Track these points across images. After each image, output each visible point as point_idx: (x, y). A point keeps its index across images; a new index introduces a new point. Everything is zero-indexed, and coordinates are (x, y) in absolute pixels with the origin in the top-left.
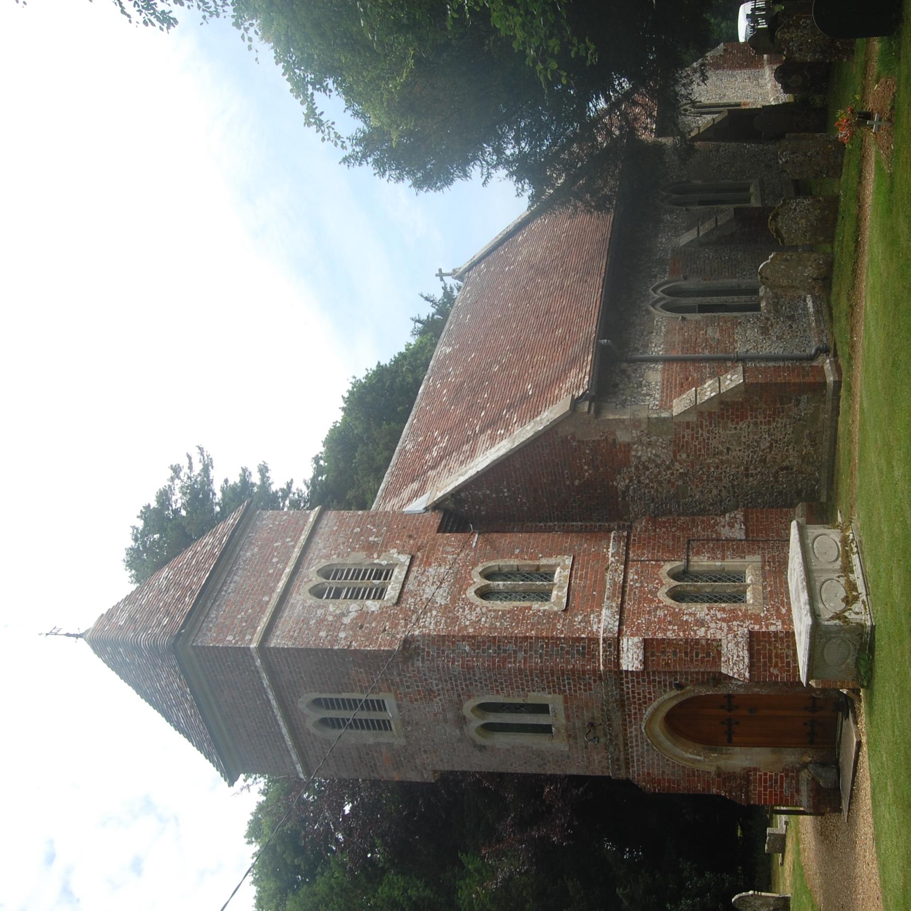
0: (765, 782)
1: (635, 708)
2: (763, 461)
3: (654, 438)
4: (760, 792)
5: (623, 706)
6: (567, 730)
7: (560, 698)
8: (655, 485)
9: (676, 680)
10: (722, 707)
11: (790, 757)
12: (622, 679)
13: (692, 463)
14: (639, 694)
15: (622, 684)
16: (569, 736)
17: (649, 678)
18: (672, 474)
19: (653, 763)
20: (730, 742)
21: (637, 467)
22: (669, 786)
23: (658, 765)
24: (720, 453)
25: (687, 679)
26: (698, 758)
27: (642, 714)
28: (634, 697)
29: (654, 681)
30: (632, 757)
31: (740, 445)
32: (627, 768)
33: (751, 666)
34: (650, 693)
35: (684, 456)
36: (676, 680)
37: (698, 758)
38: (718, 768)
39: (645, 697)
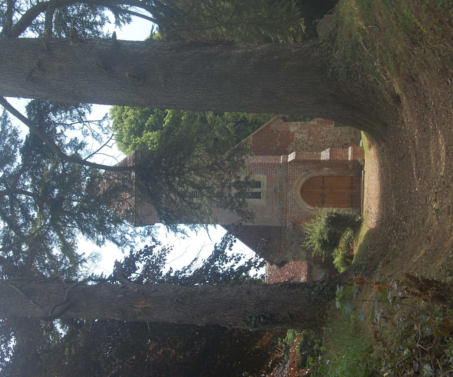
2: (338, 141)
3: (302, 130)
5: (287, 181)
6: (266, 194)
7: (266, 176)
8: (301, 150)
10: (321, 188)
13: (314, 141)
16: (267, 197)
18: (308, 146)
21: (296, 142)
23: (297, 212)
24: (324, 137)
26: (312, 208)
27: (293, 185)
31: (330, 134)
32: (286, 214)
33: (330, 156)
35: (312, 138)
37: (312, 208)
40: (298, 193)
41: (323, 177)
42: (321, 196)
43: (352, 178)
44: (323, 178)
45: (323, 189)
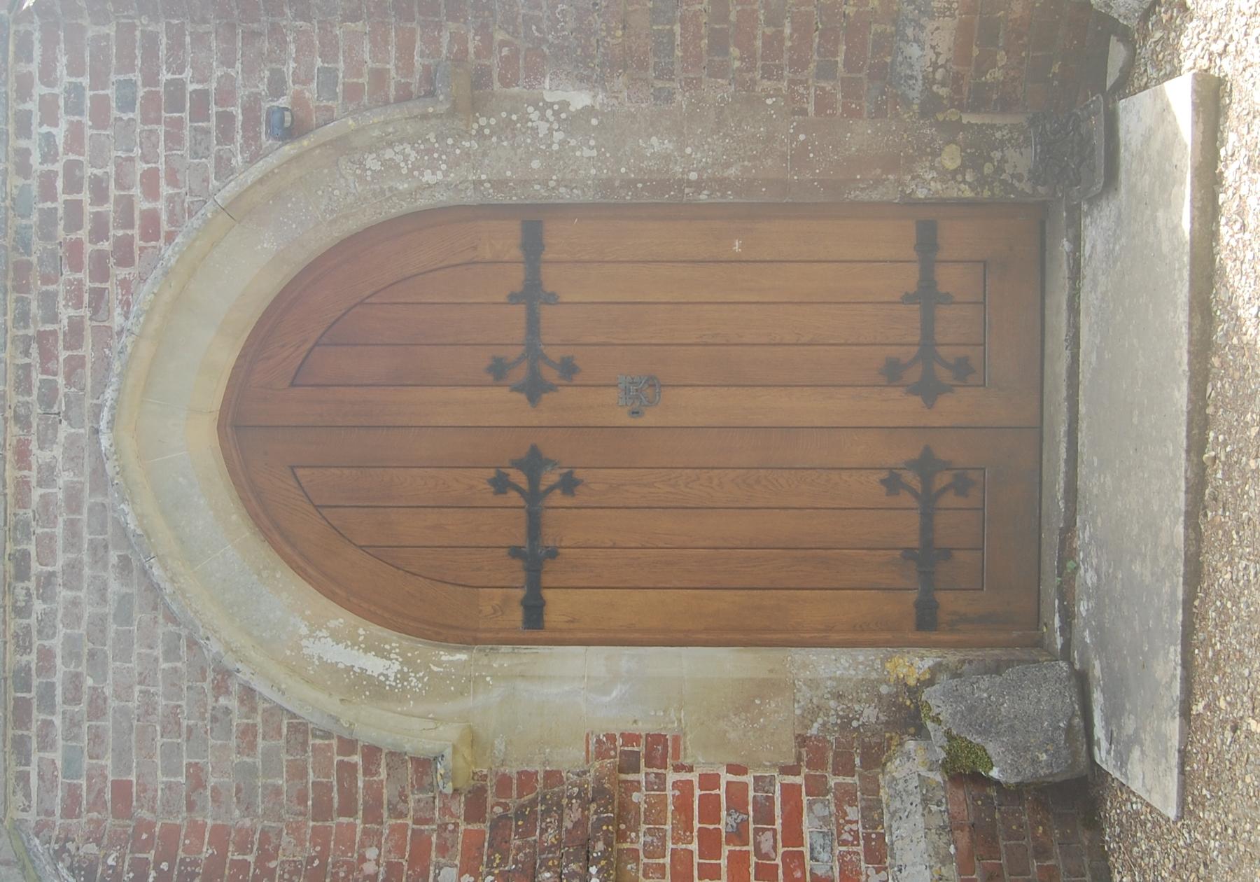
0: (710, 810)
1: (75, 297)
4: (683, 859)
9: (277, 87)
10: (498, 371)
11: (832, 671)
12: (24, 92)
14: (100, 194)
15: (24, 128)
17: (151, 78)
19: (148, 708)
20: (535, 622)
22: (217, 862)
23: (172, 721)
25: (329, 78)
28: (74, 209)
29: (176, 88)
30: (46, 655)
34: (151, 190)
36: (277, 87)
37: (374, 665)
38: (474, 740)
39: (126, 205)
40: (187, 440)
41: (533, 223)
42: (501, 484)
43: (927, 229)
44: (533, 243)
45: (534, 389)
